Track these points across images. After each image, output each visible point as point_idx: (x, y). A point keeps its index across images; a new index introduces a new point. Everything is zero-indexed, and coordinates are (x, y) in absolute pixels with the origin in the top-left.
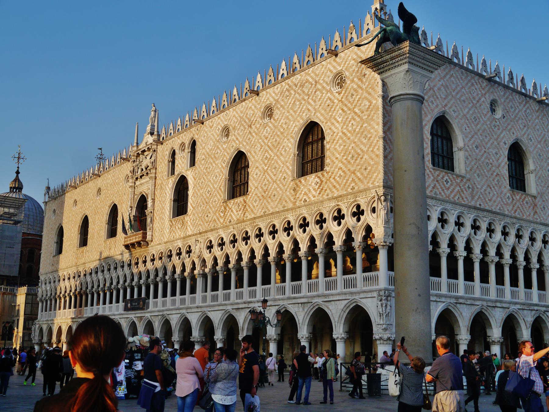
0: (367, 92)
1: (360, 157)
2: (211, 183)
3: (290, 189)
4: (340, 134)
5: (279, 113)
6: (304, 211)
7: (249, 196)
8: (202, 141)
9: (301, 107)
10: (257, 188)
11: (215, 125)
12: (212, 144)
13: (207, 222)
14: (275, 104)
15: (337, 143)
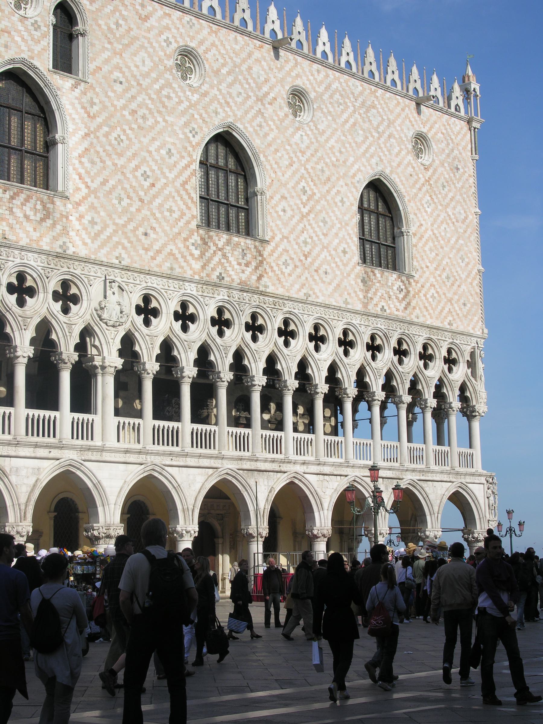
0: (461, 195)
1: (458, 283)
2: (156, 161)
3: (357, 276)
4: (430, 232)
5: (326, 123)
6: (379, 326)
7: (269, 248)
8: (109, 28)
9: (367, 143)
10: (287, 238)
11: (152, 21)
12: (148, 62)
13: (147, 250)
14: (316, 98)
15: (426, 243)
